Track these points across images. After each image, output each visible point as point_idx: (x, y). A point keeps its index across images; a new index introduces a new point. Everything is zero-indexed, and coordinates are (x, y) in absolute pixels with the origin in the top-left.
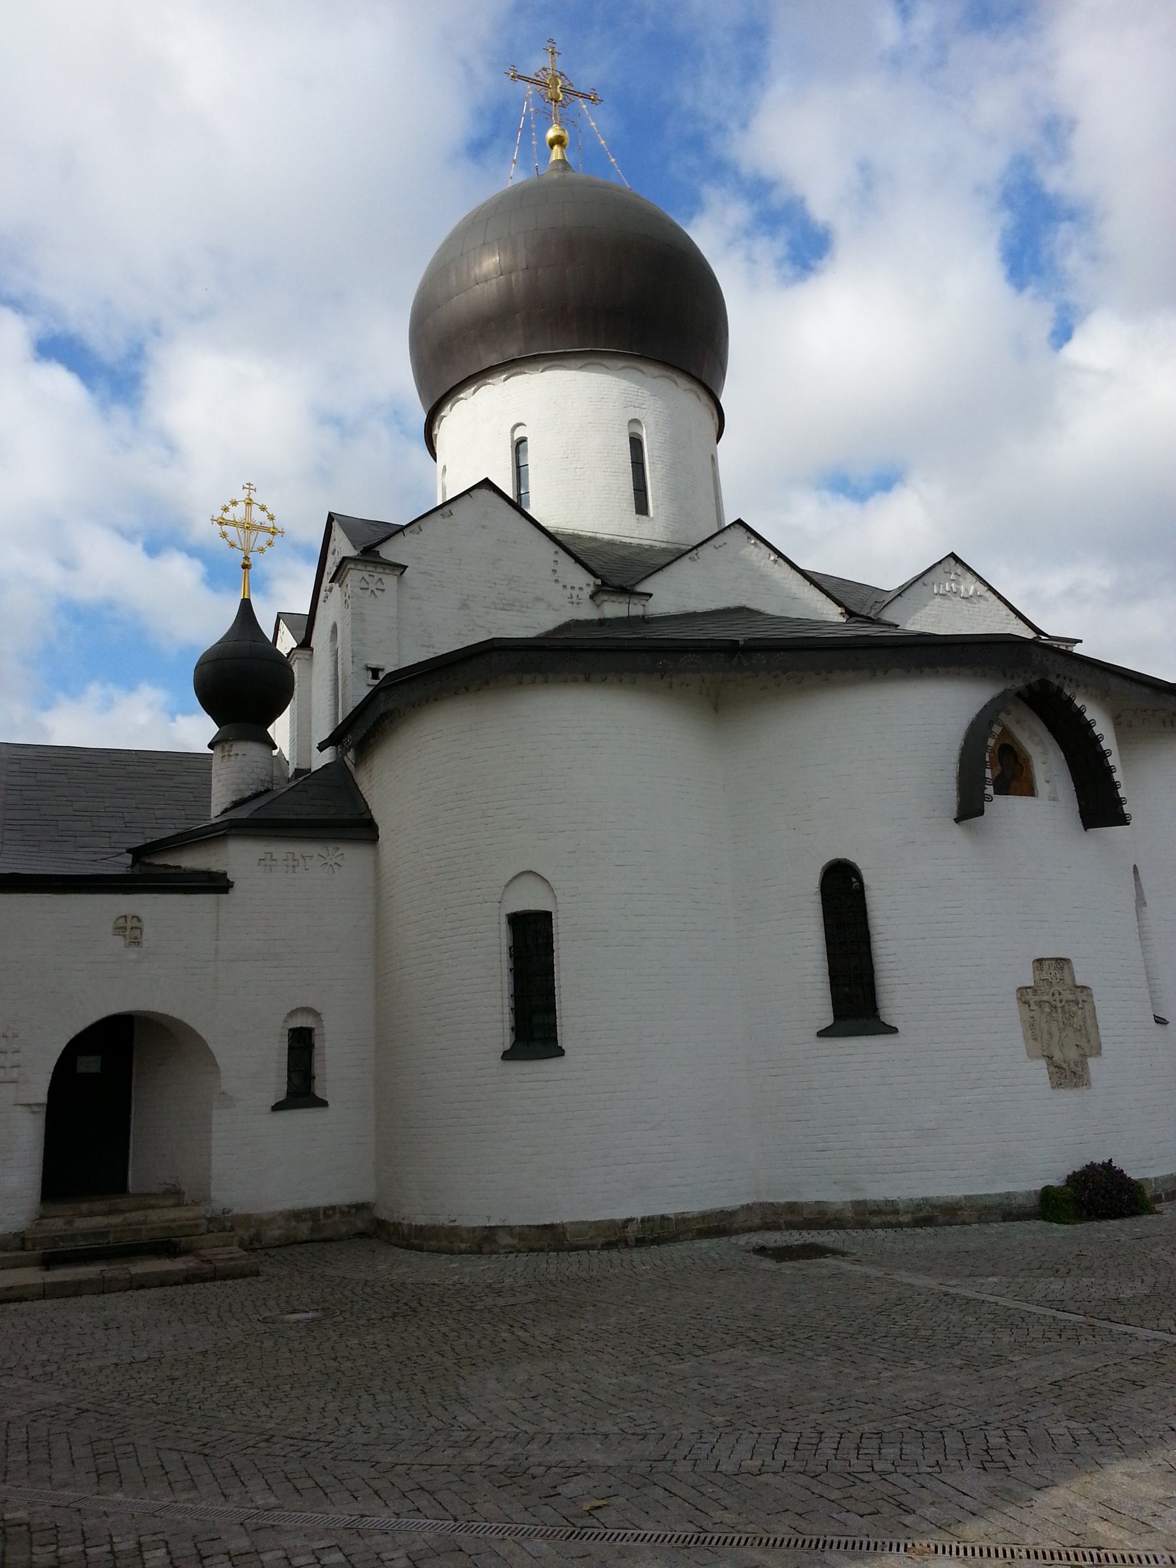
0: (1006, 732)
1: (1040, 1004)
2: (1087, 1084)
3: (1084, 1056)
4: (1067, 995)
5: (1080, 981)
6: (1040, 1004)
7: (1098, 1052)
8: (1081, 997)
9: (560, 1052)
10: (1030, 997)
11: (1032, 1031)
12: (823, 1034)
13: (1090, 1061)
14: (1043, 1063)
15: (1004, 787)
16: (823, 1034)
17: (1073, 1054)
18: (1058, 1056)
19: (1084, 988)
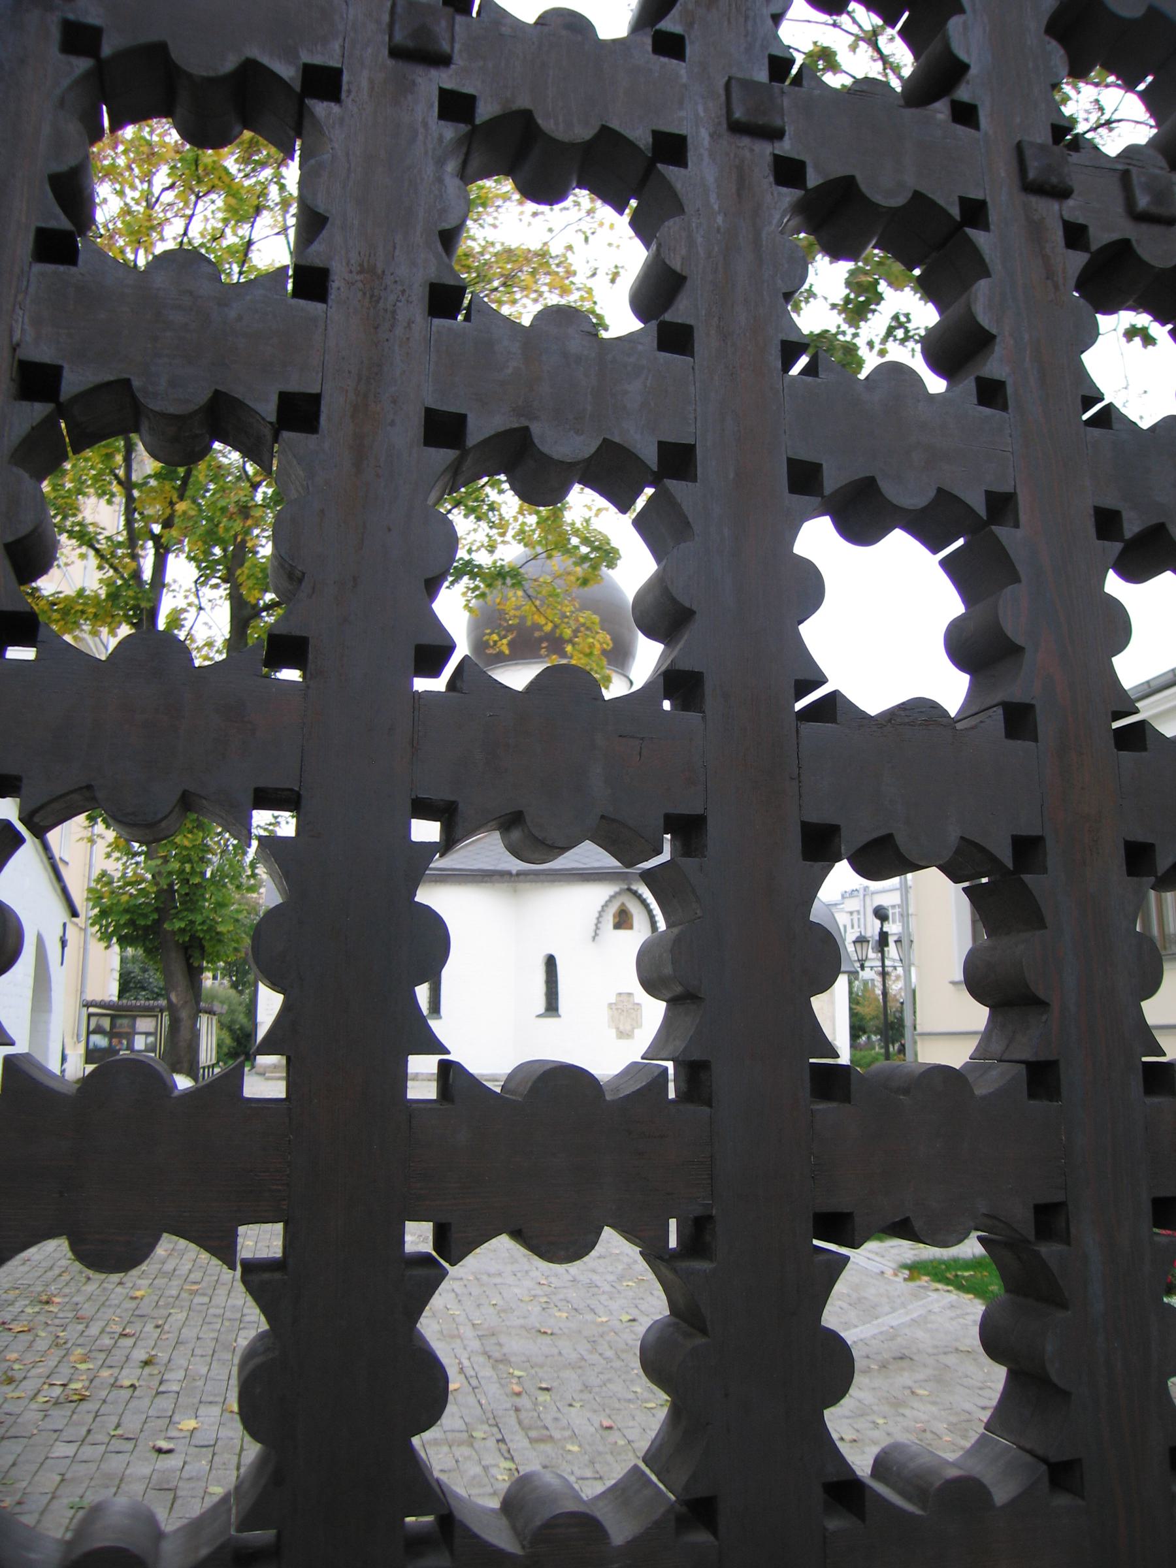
0: (623, 904)
1: (617, 1009)
2: (633, 1038)
3: (633, 1028)
4: (630, 1006)
5: (636, 1001)
6: (617, 1009)
7: (640, 1026)
8: (636, 1007)
9: (441, 1018)
10: (613, 1006)
11: (612, 1018)
12: (539, 1016)
13: (636, 1031)
14: (614, 1030)
15: (617, 926)
16: (539, 1016)
17: (628, 1028)
18: (621, 1028)
19: (638, 1004)
